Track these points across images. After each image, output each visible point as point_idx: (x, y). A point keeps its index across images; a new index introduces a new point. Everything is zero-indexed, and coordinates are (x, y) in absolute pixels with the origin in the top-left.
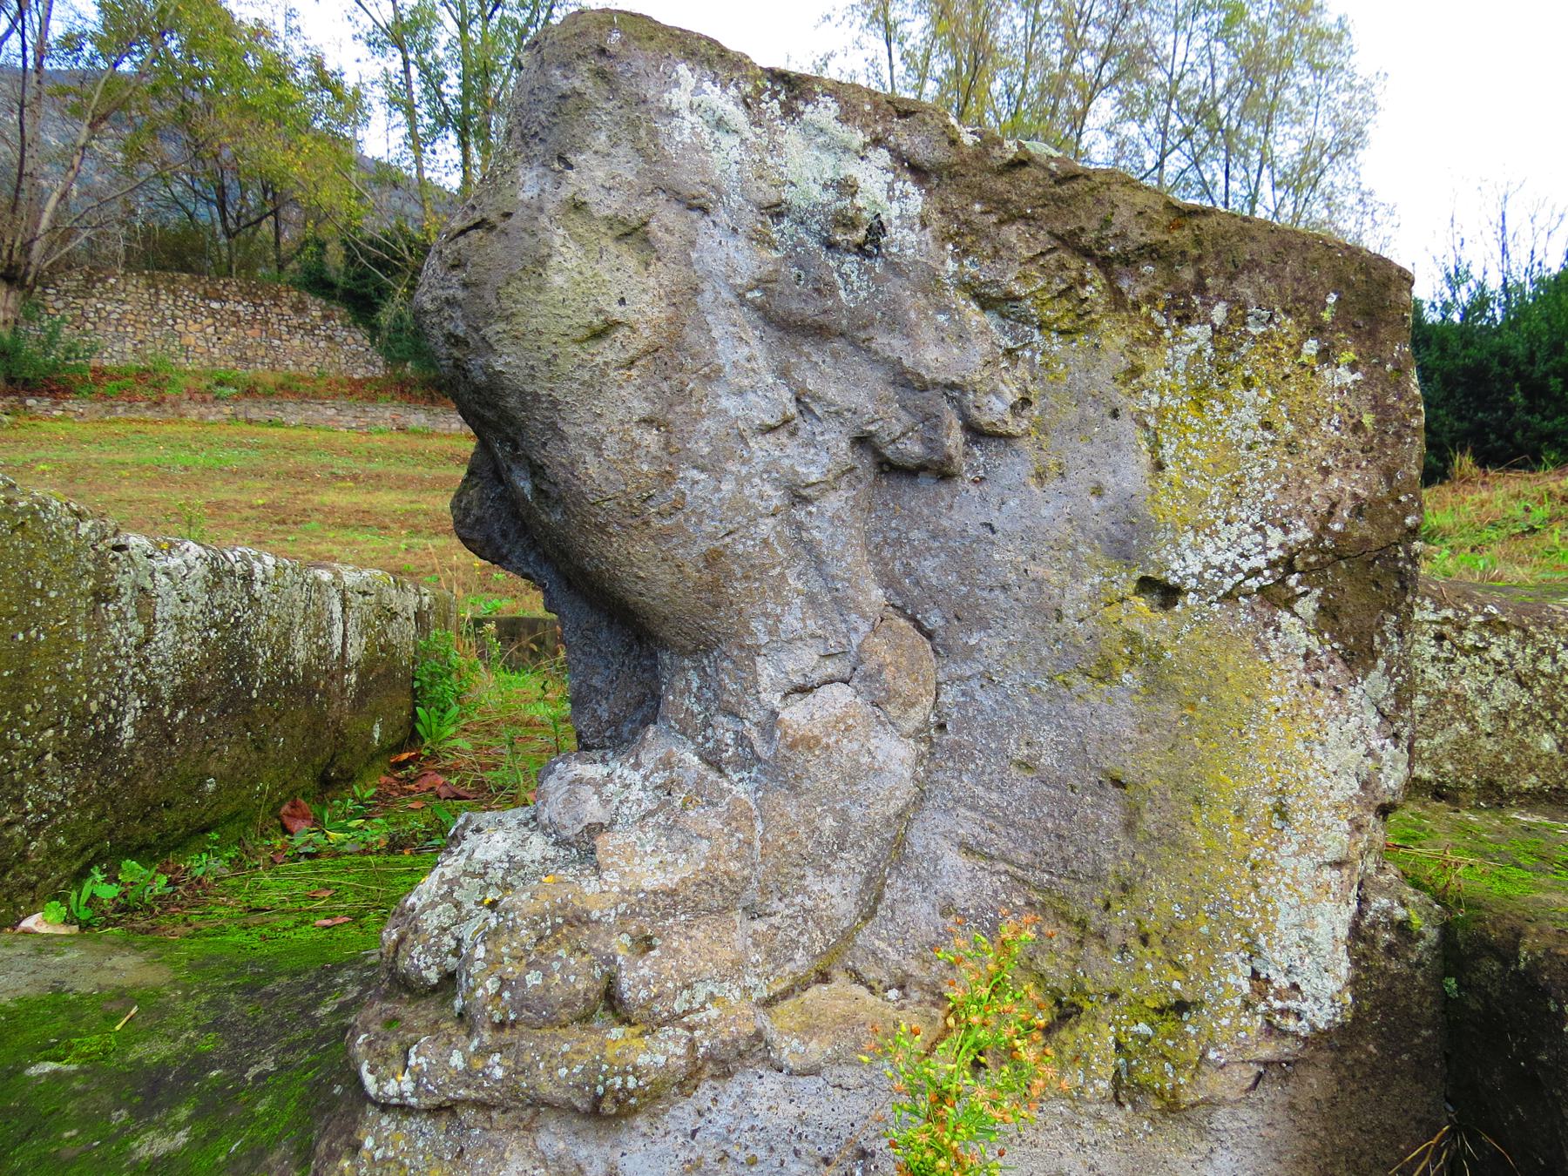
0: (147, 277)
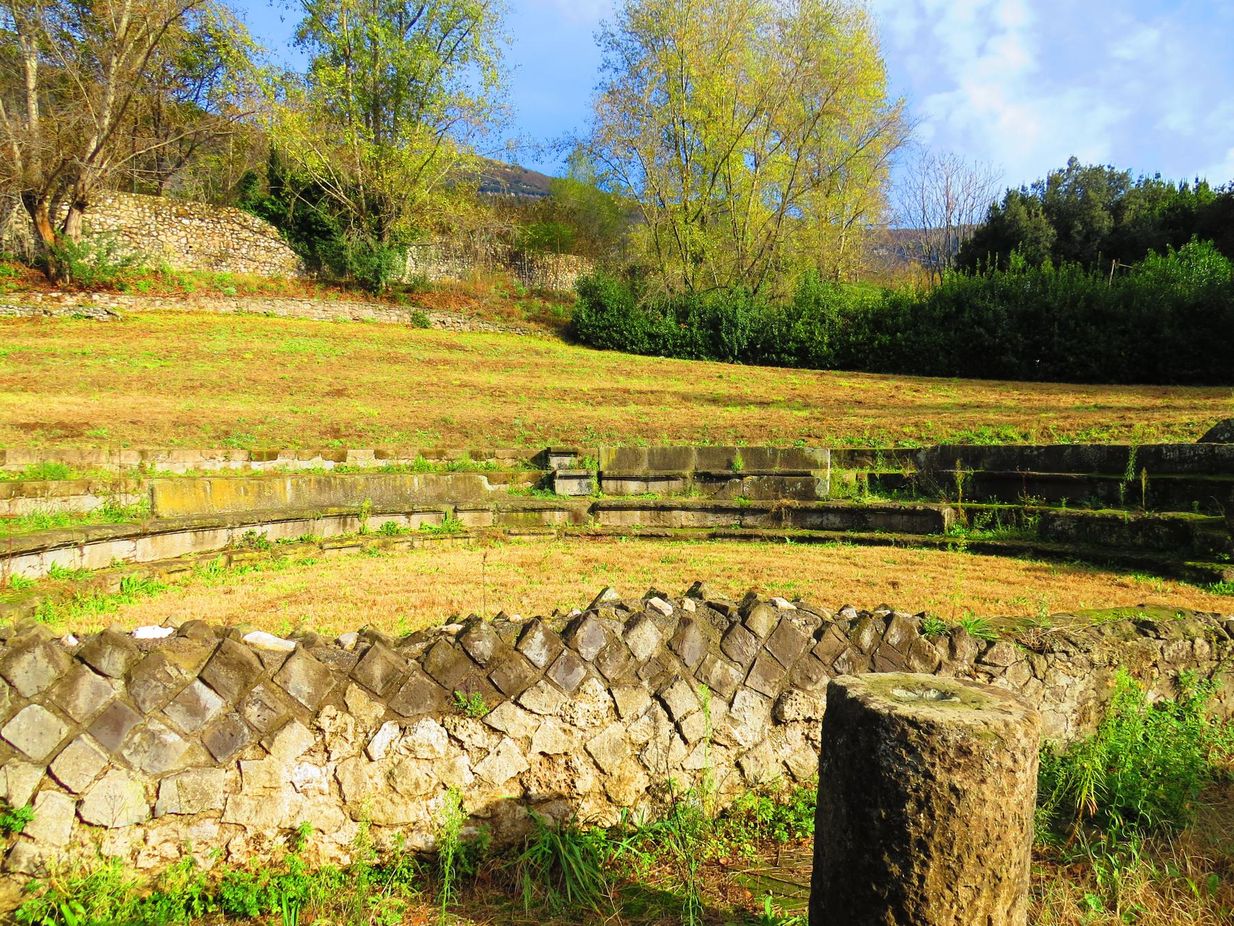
0: (134, 199)
